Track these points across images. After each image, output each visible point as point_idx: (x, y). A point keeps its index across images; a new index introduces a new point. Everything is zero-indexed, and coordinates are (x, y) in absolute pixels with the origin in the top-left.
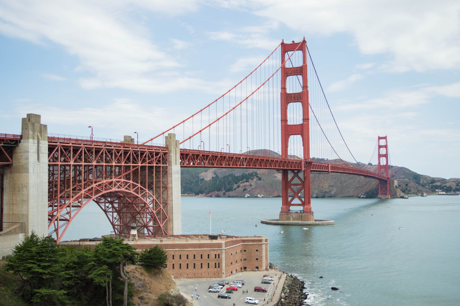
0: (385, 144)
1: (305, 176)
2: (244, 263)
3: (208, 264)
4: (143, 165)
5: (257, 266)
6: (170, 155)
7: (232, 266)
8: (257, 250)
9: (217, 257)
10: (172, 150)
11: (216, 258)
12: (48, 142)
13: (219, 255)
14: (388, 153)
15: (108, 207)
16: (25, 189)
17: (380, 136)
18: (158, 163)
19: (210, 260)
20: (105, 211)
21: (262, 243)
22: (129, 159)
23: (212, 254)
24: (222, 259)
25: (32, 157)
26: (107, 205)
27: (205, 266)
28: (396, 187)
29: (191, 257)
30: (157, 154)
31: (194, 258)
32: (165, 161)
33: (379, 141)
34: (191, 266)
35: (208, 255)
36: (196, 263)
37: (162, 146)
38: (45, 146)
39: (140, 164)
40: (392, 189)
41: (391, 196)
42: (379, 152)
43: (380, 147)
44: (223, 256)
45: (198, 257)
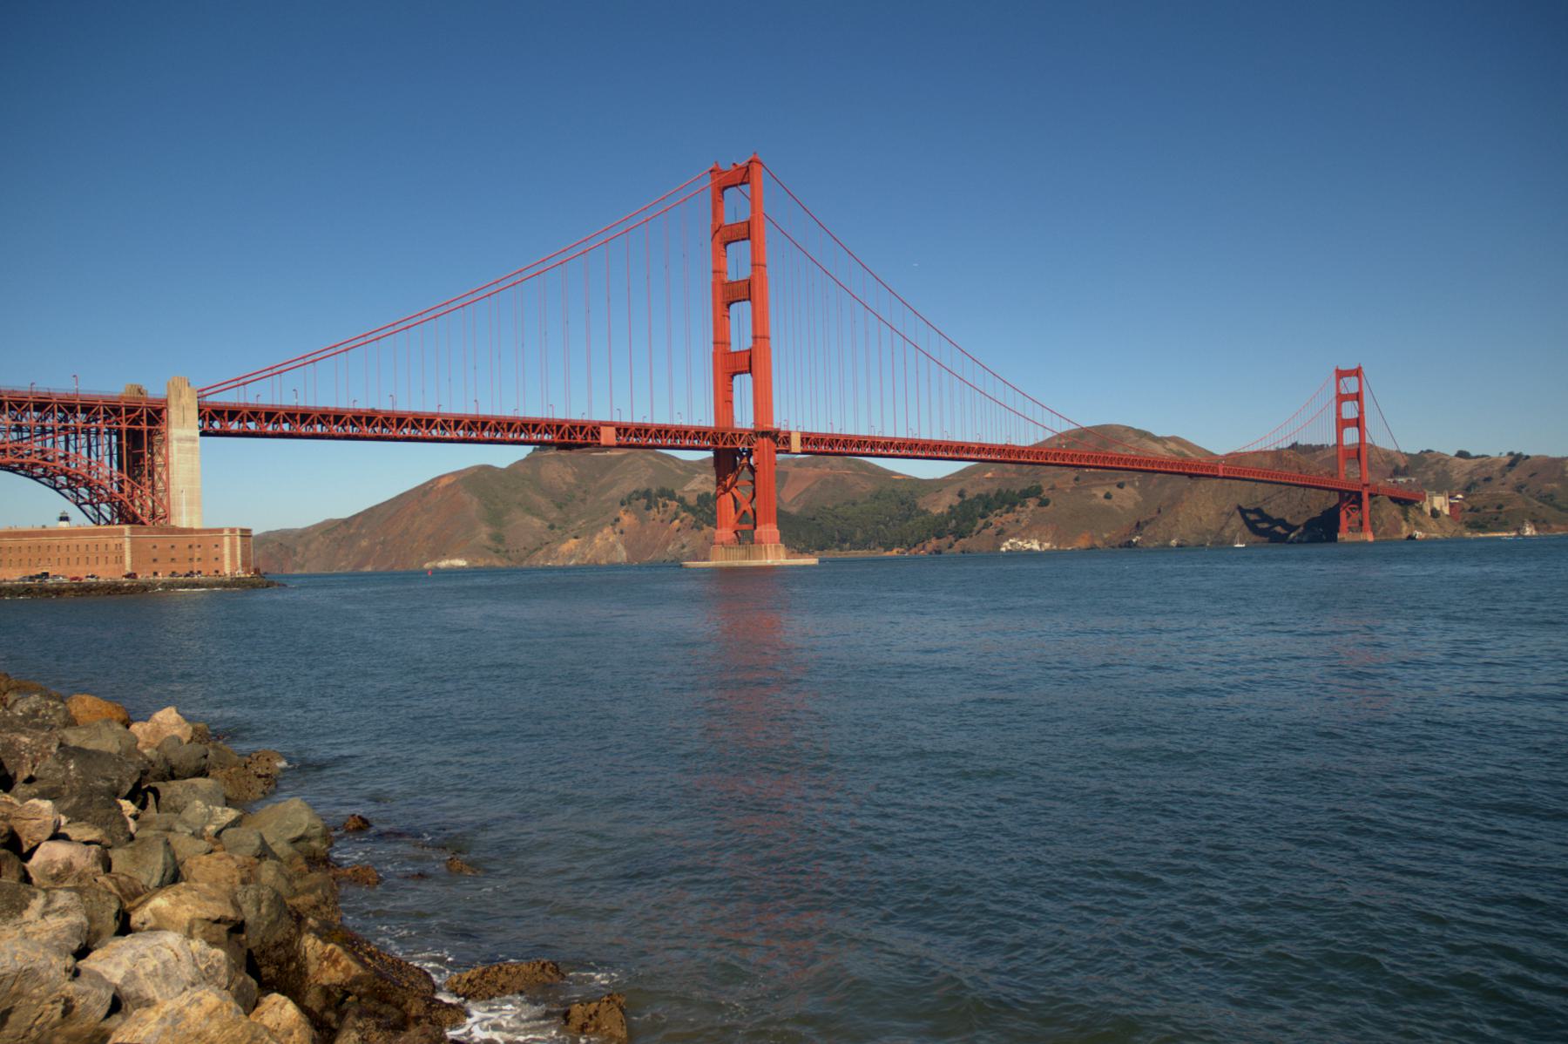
29: (82, 548)
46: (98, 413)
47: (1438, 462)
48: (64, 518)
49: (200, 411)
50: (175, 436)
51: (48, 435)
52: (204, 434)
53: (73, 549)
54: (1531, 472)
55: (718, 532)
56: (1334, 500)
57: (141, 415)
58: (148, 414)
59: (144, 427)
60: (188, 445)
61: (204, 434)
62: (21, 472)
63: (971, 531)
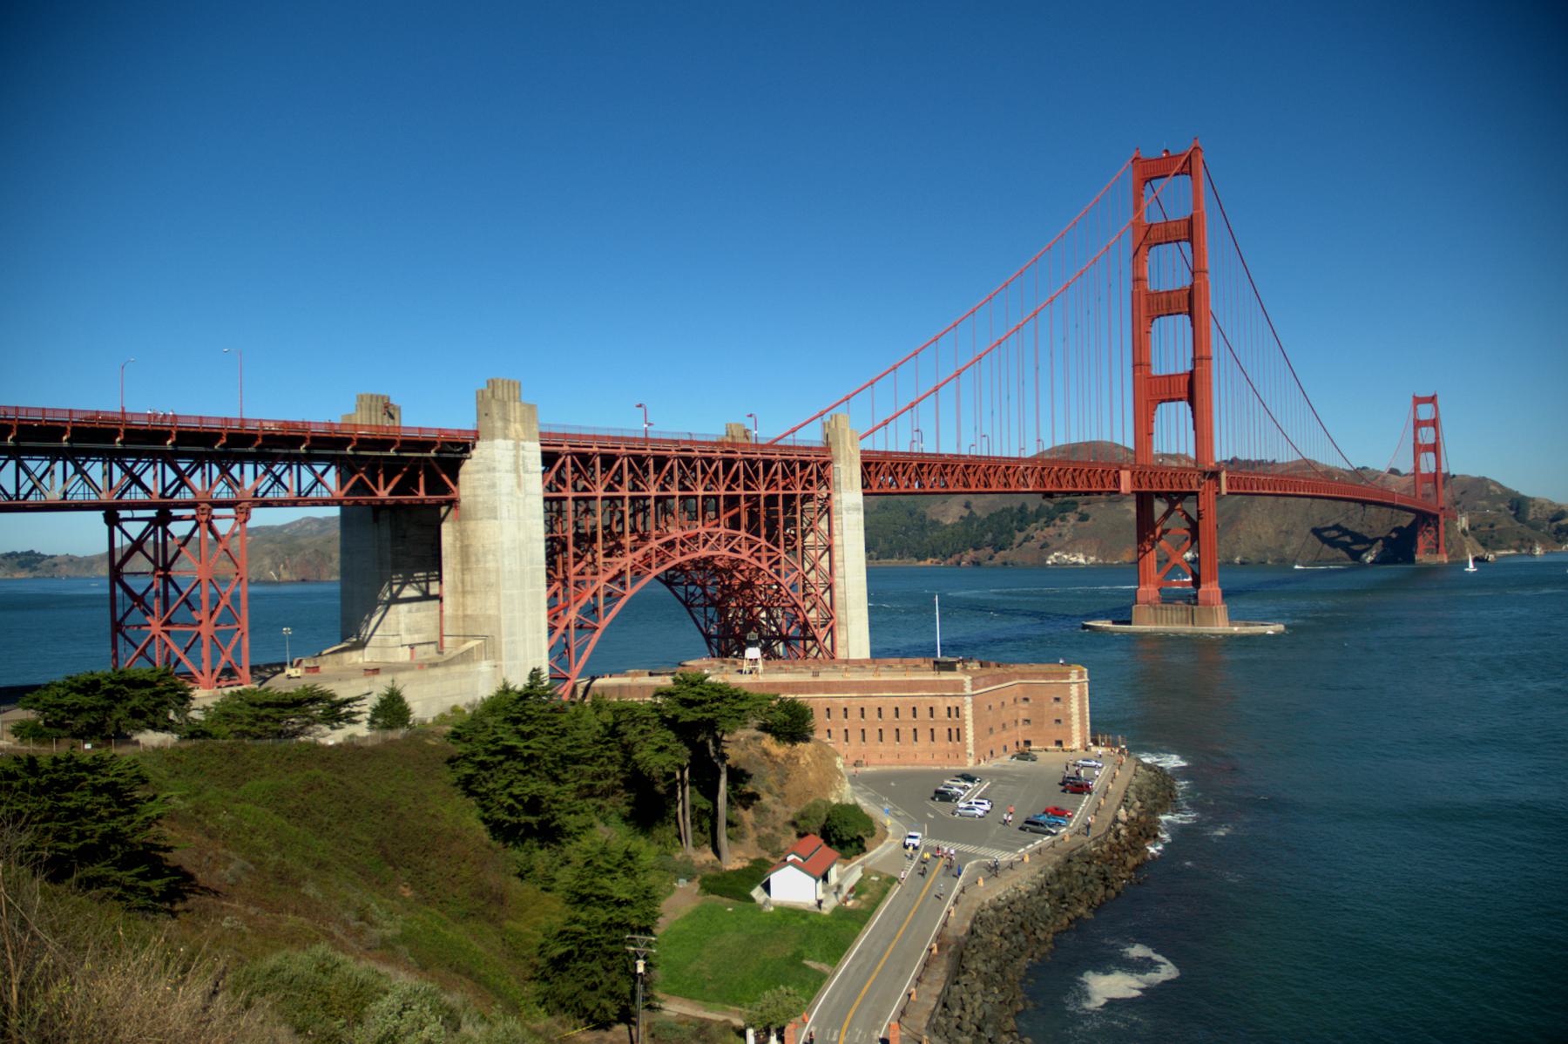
0: (1433, 417)
1: (1200, 508)
3: (932, 730)
4: (771, 492)
5: (1058, 739)
6: (836, 466)
7: (992, 739)
8: (1057, 699)
9: (953, 713)
10: (842, 455)
11: (950, 716)
12: (542, 445)
13: (957, 708)
14: (1441, 440)
15: (693, 594)
16: (490, 557)
17: (1420, 394)
18: (807, 485)
19: (936, 721)
20: (688, 605)
21: (1071, 681)
22: (735, 478)
24: (965, 720)
25: (506, 481)
26: (691, 589)
27: (924, 736)
28: (1463, 531)
29: (889, 713)
30: (804, 465)
31: (897, 716)
32: (824, 480)
33: (1415, 409)
34: (889, 735)
35: (931, 709)
36: (902, 729)
37: (818, 445)
38: (534, 452)
39: (763, 492)
40: (1451, 537)
41: (1448, 558)
42: (1416, 439)
43: (1418, 424)
44: (968, 712)
45: (906, 714)
47: (1377, 477)
53: (871, 714)
54: (1461, 491)
55: (1142, 589)
56: (1406, 520)
63: (1011, 544)
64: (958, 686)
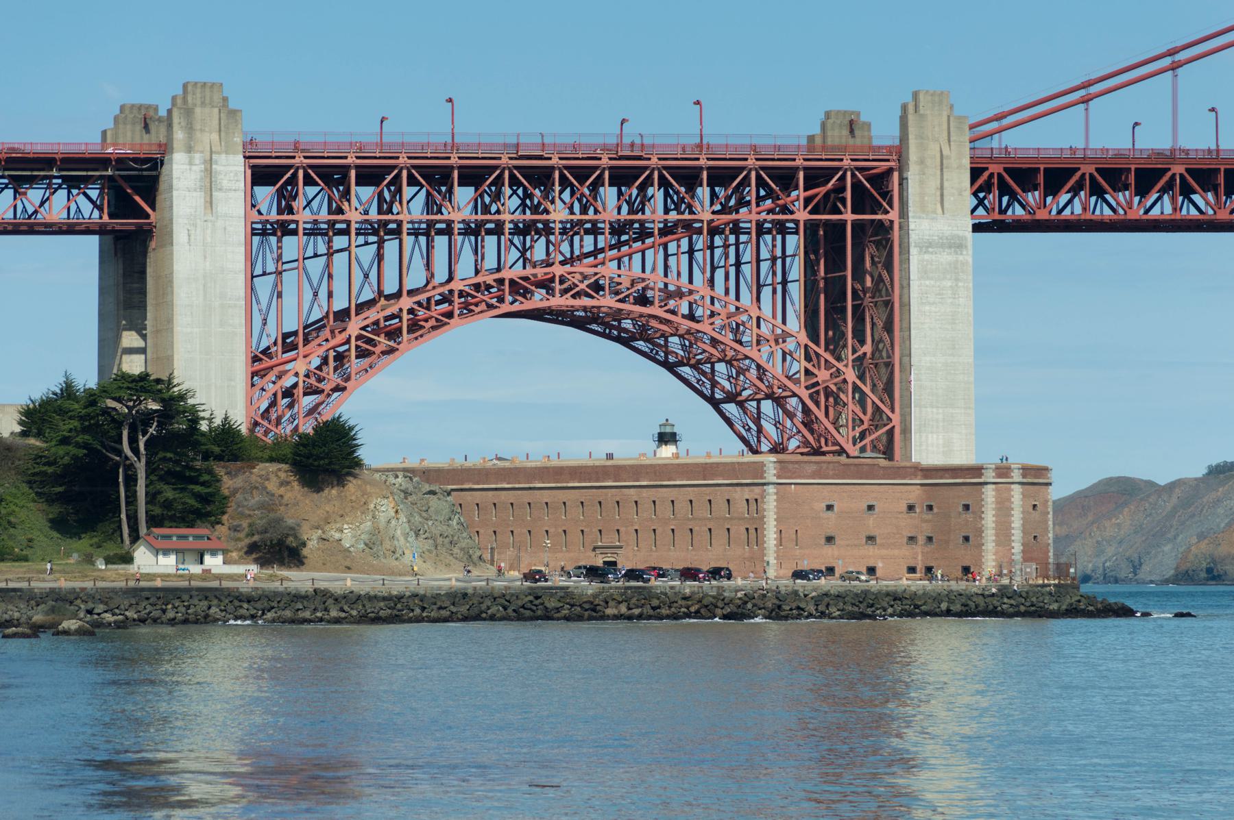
2: (927, 553)
9: (753, 506)
23: (737, 497)
27: (720, 537)
46: (745, 182)
48: (666, 438)
49: (975, 173)
50: (913, 237)
51: (649, 241)
52: (977, 228)
57: (843, 189)
58: (857, 185)
59: (849, 216)
60: (946, 257)
61: (977, 228)
62: (594, 327)
64: (759, 469)
